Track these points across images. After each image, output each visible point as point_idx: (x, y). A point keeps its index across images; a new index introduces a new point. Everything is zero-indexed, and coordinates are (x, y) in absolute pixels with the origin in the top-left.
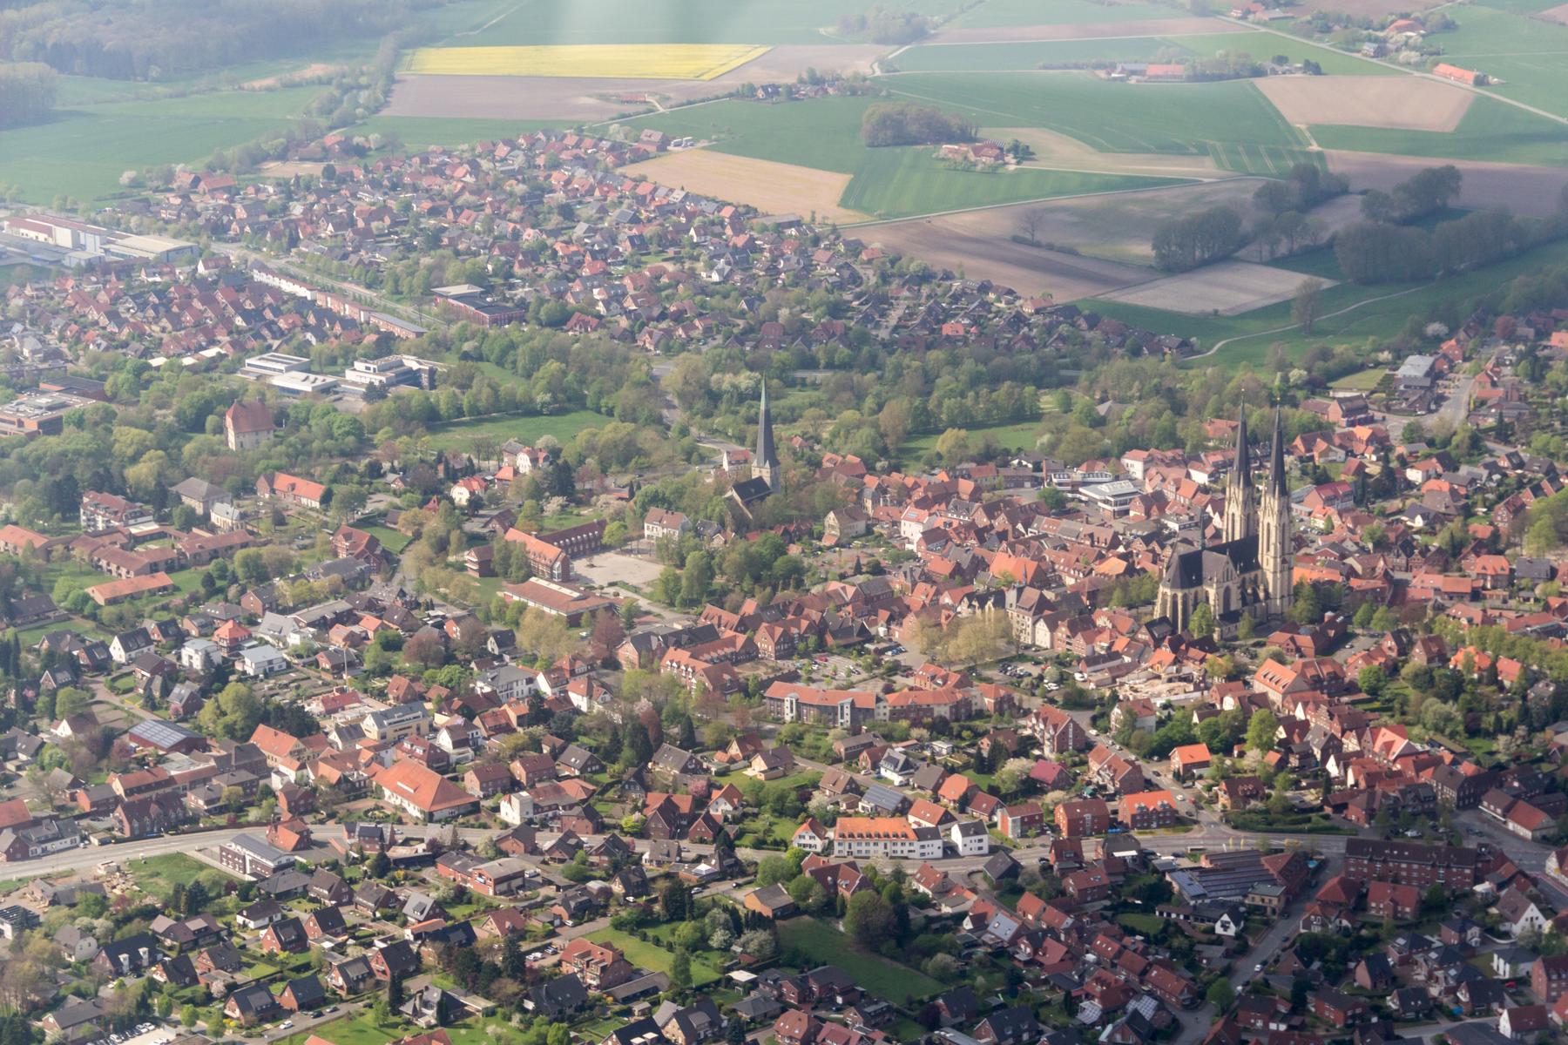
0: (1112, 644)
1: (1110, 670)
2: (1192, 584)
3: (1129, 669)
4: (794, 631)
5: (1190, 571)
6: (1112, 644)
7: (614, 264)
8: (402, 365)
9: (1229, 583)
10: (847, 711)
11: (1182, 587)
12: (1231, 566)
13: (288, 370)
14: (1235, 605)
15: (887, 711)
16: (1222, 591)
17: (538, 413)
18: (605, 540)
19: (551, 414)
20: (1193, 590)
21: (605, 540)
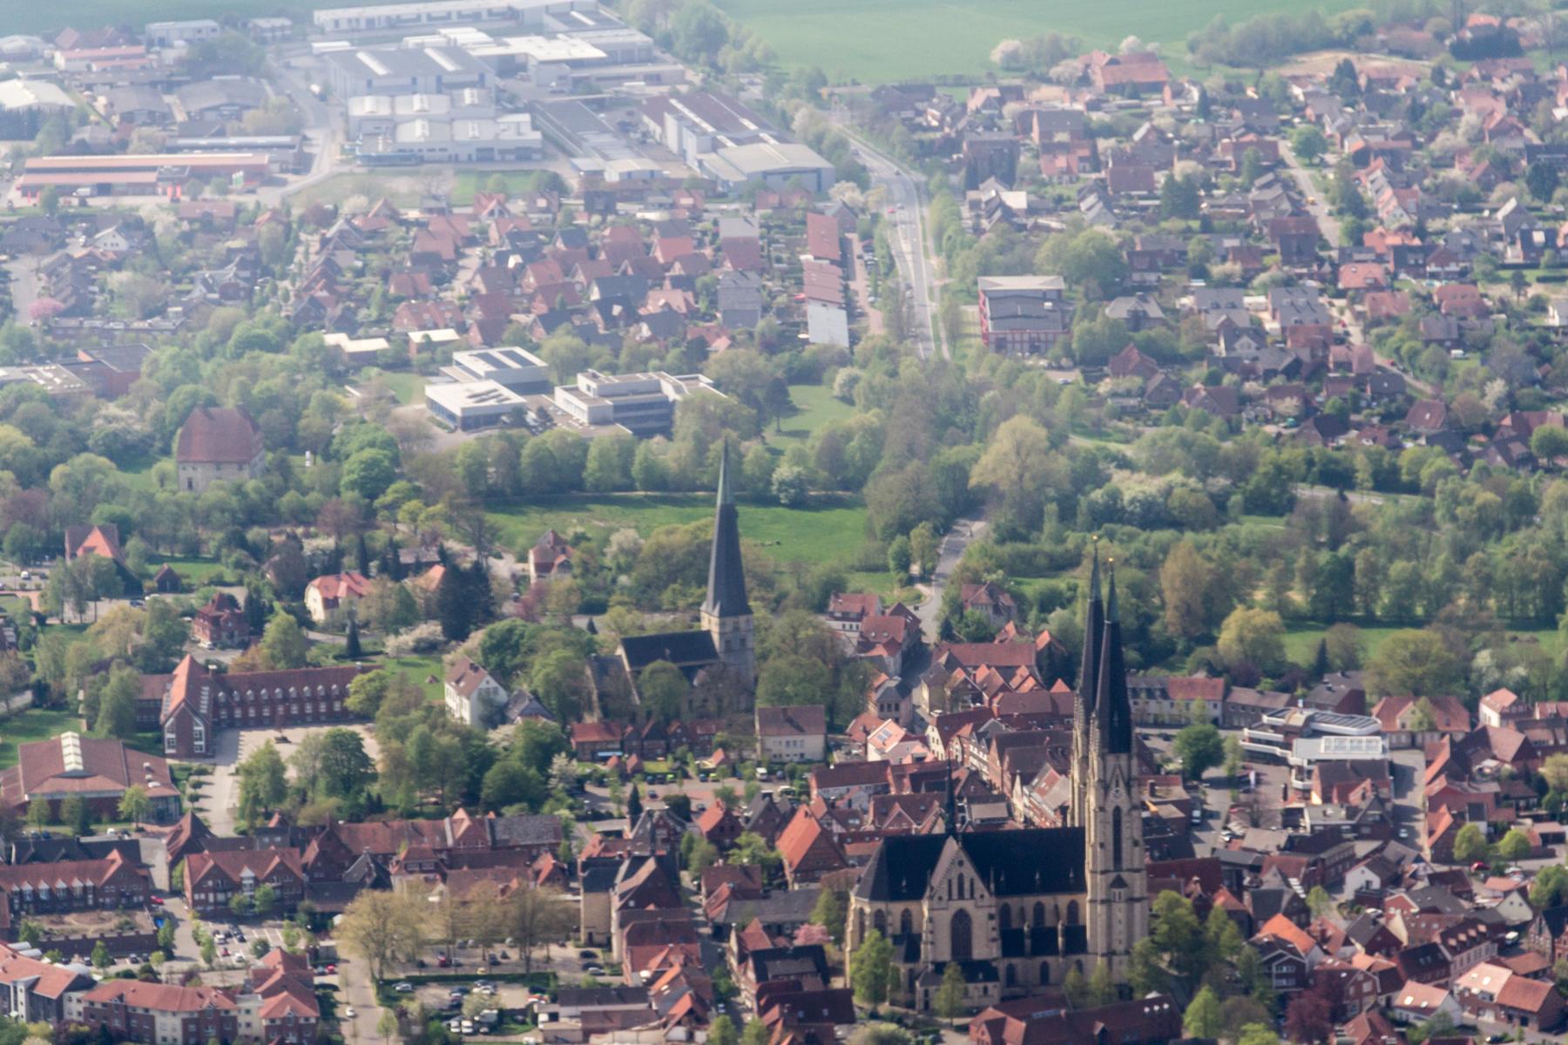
0: (657, 976)
1: (584, 1016)
2: (895, 896)
3: (627, 1022)
4: (247, 873)
5: (904, 869)
6: (657, 976)
7: (1434, 276)
8: (659, 391)
9: (968, 905)
10: (22, 997)
11: (875, 896)
12: (969, 871)
13: (489, 376)
14: (984, 947)
15: (80, 1008)
16: (945, 917)
17: (773, 502)
18: (352, 702)
19: (798, 503)
20: (897, 908)
21: (352, 702)
